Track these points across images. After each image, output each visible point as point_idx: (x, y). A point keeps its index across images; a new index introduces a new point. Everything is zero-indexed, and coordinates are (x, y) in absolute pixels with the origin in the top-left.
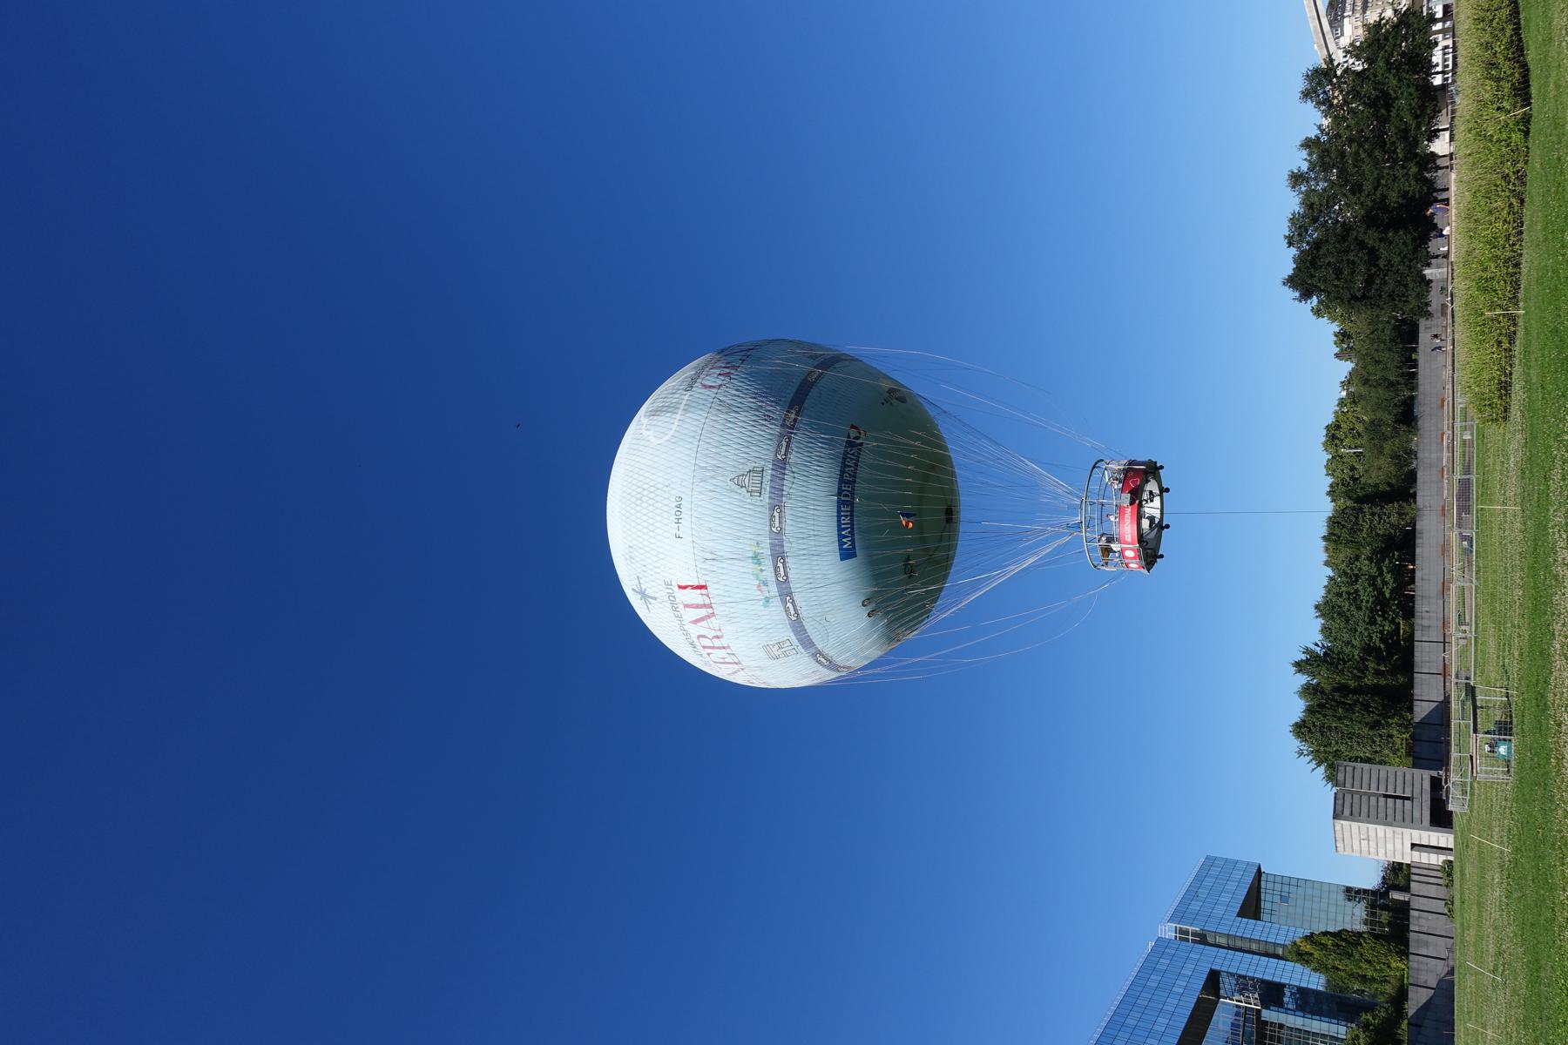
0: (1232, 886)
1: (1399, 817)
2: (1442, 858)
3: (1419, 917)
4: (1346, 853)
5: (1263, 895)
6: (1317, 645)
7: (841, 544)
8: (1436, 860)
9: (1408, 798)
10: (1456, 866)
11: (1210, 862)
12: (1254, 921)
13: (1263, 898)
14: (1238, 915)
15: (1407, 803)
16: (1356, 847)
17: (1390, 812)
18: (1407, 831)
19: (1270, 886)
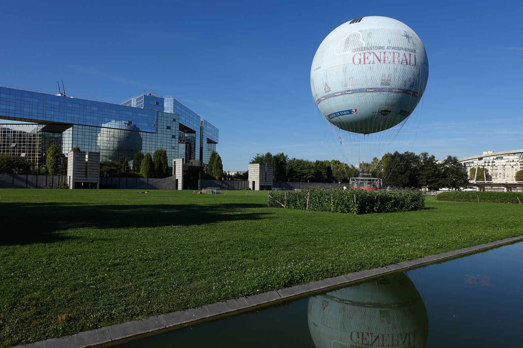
0: (213, 136)
1: (262, 179)
2: (251, 188)
3: (237, 183)
4: (249, 166)
5: (210, 144)
6: (288, 159)
8: (251, 186)
9: (266, 180)
10: (250, 191)
11: (217, 130)
12: (206, 142)
13: (209, 144)
14: (207, 138)
15: (265, 181)
16: (251, 169)
17: (263, 177)
18: (259, 180)
19: (213, 146)
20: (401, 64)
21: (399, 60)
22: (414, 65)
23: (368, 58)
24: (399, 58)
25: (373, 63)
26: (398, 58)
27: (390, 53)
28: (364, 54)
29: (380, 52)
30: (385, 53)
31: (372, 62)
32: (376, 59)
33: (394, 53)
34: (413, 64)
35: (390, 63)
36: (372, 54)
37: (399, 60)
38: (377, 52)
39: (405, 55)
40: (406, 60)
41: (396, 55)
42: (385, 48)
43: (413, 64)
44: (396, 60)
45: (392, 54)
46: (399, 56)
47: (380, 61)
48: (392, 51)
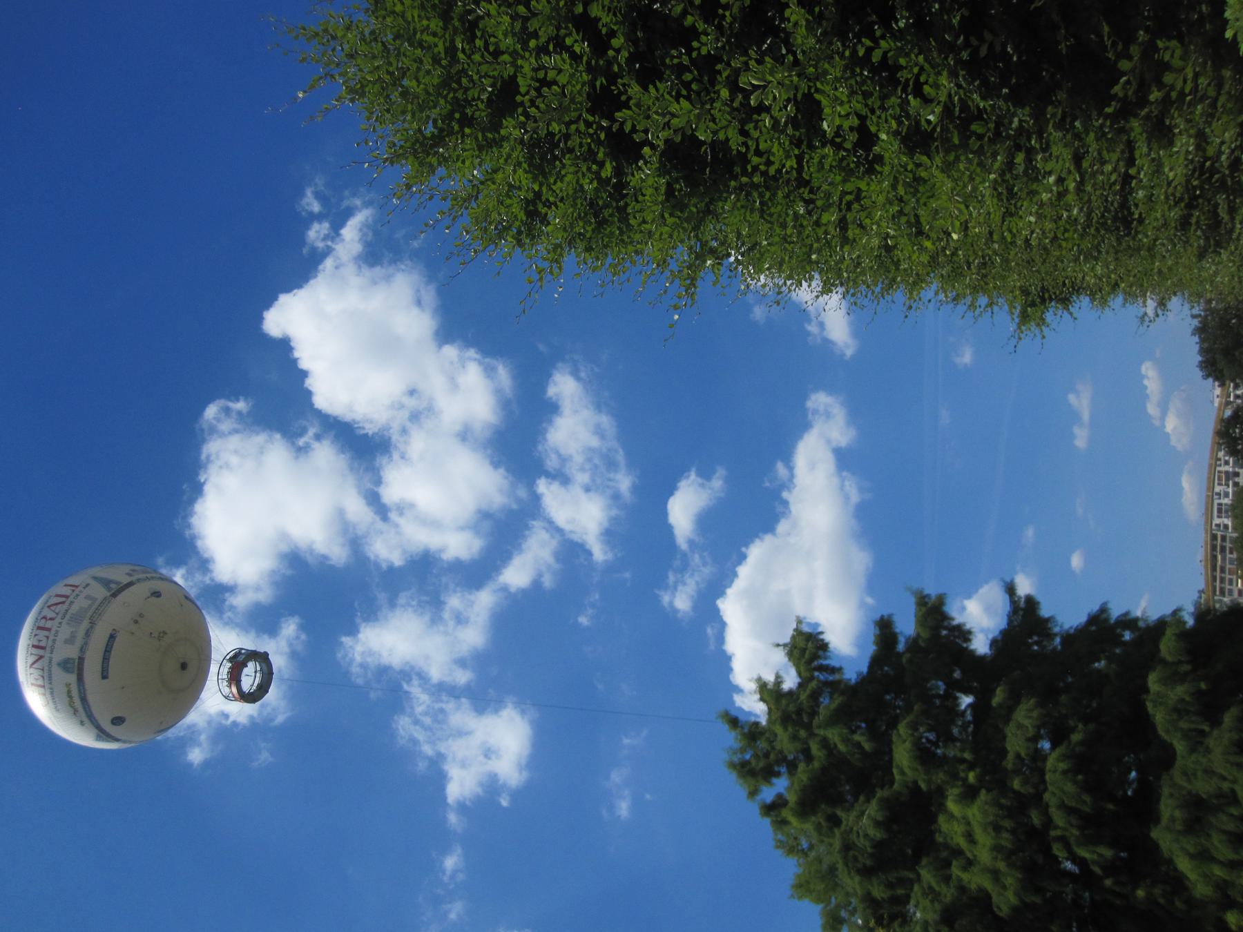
7: (102, 673)
20: (57, 614)
22: (73, 588)
25: (43, 670)
35: (47, 637)
40: (56, 604)
44: (49, 624)
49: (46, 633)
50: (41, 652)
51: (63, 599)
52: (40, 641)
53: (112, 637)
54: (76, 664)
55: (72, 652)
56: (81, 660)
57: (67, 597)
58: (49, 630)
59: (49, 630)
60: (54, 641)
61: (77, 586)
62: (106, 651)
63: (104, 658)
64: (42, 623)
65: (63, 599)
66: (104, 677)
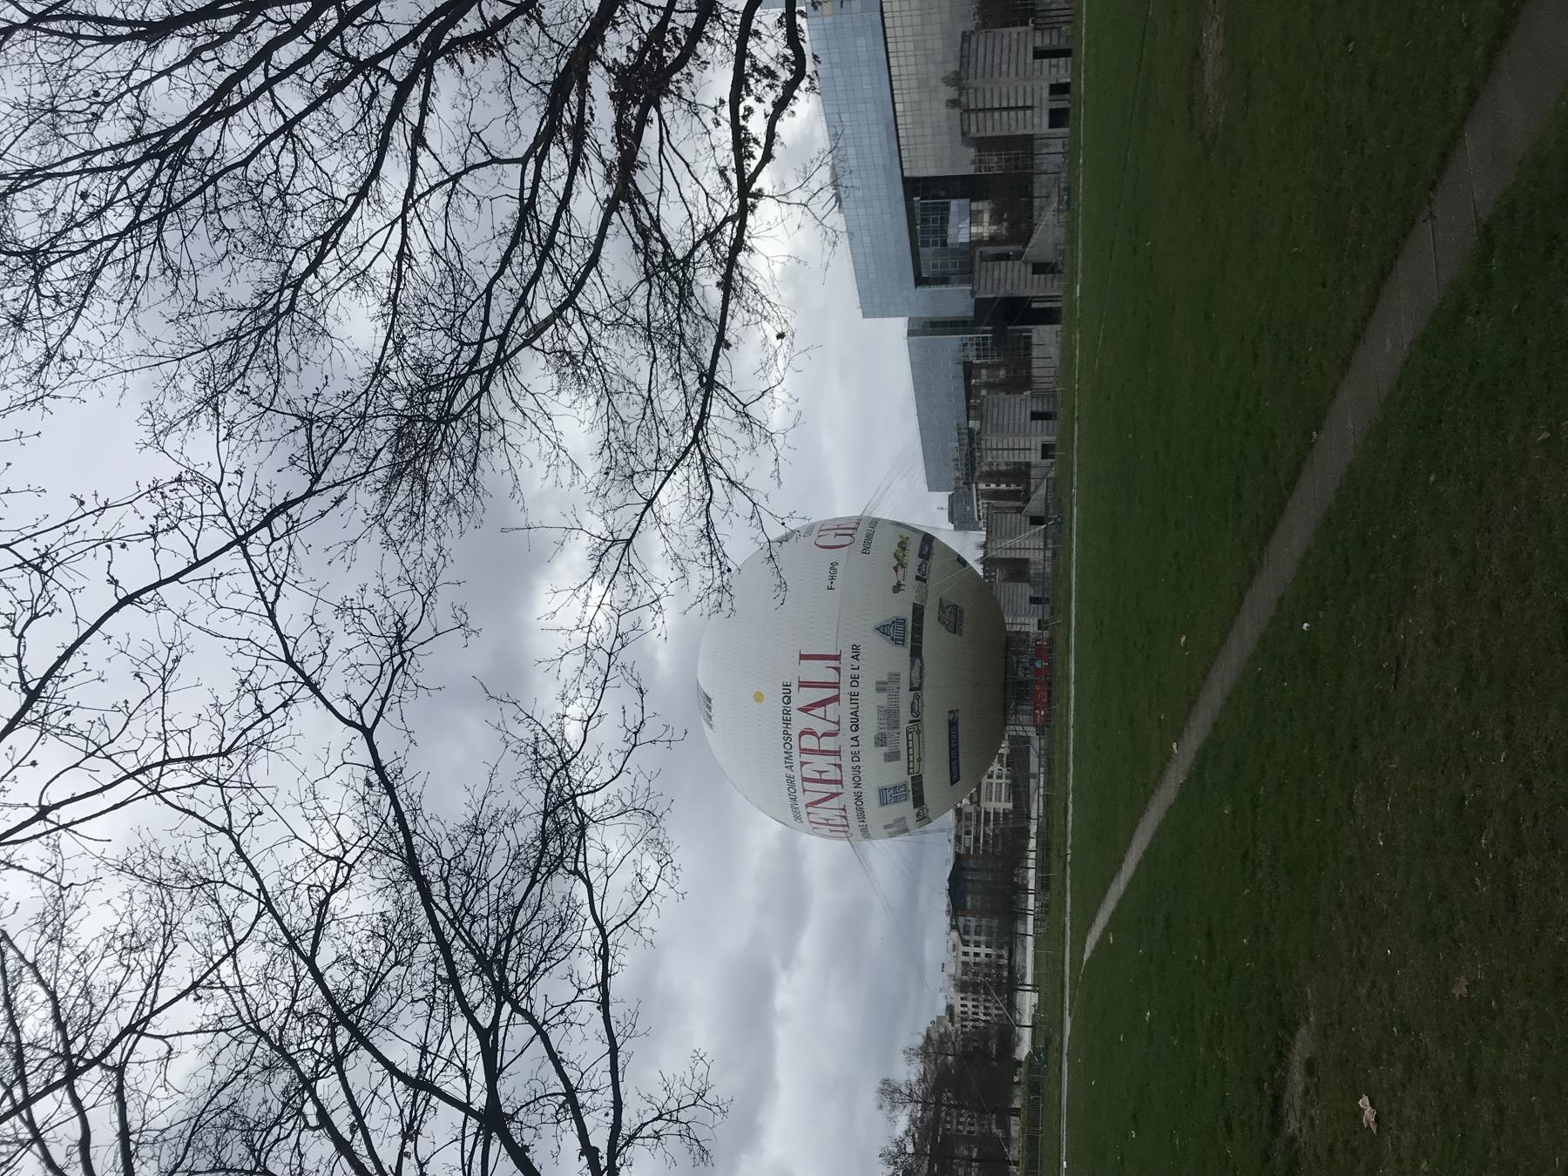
20: (838, 723)
21: (824, 735)
23: (827, 820)
24: (819, 735)
25: (844, 809)
26: (819, 739)
27: (803, 764)
28: (810, 822)
29: (804, 791)
30: (805, 779)
31: (843, 813)
32: (834, 803)
33: (804, 751)
34: (835, 668)
35: (839, 766)
36: (810, 809)
37: (824, 735)
38: (804, 800)
39: (805, 710)
40: (823, 703)
41: (809, 742)
42: (789, 772)
43: (835, 668)
44: (827, 743)
45: (805, 758)
46: (813, 733)
47: (833, 795)
48: (797, 758)
49: (832, 759)
50: (833, 788)
51: (831, 693)
52: (821, 772)
53: (953, 725)
54: (910, 788)
55: (897, 774)
56: (917, 781)
57: (835, 685)
58: (837, 753)
59: (837, 753)
60: (857, 769)
61: (837, 658)
62: (951, 749)
63: (951, 760)
64: (809, 742)
65: (831, 693)
66: (953, 781)
